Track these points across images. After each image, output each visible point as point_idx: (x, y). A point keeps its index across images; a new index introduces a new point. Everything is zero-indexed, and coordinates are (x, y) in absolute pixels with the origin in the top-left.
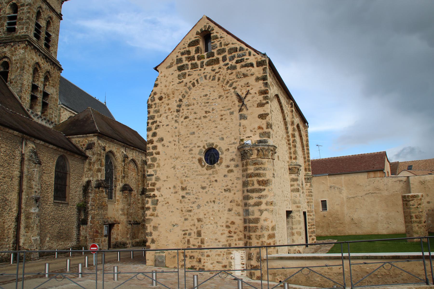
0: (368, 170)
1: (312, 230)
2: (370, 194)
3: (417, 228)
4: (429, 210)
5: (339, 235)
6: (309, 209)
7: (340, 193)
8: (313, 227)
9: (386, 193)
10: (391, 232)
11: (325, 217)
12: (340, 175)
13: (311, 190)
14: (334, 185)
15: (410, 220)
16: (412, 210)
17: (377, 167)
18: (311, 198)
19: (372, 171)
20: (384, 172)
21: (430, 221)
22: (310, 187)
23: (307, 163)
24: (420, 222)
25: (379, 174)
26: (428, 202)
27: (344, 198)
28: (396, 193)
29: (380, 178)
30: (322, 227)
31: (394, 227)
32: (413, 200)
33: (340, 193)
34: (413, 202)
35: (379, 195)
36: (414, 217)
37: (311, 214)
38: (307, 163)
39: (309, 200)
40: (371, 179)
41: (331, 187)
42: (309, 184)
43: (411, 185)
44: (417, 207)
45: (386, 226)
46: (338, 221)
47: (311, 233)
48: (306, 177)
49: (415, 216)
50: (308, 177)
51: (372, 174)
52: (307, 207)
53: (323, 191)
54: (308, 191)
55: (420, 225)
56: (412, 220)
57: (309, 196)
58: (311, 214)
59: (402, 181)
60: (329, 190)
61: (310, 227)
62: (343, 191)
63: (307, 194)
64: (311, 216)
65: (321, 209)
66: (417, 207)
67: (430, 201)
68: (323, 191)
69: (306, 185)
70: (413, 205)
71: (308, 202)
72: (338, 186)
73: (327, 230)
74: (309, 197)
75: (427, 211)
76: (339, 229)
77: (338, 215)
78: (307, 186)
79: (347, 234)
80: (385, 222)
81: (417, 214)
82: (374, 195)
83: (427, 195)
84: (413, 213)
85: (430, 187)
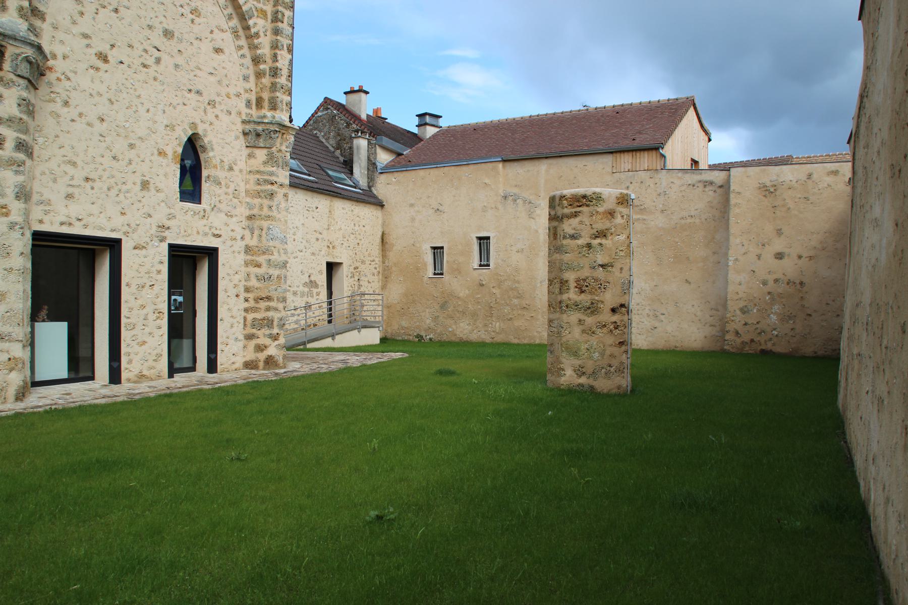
0: (616, 147)
1: (259, 316)
3: (577, 332)
4: (776, 281)
5: (516, 341)
6: (253, 242)
7: (531, 216)
8: (263, 305)
9: (658, 221)
10: (661, 345)
11: (482, 285)
12: (536, 163)
13: (272, 174)
14: (515, 191)
15: (559, 298)
16: (567, 257)
17: (643, 140)
18: (266, 202)
19: (628, 151)
20: (663, 156)
21: (774, 317)
22: (265, 163)
23: (266, 81)
24: (592, 309)
25: (646, 160)
26: (779, 256)
27: (540, 231)
28: (689, 220)
29: (649, 173)
30: (474, 315)
31: (669, 329)
32: (575, 215)
33: (531, 216)
34: (574, 222)
36: (572, 284)
37: (261, 259)
38: (266, 81)
39: (255, 211)
40: (623, 176)
41: (505, 197)
42: (261, 154)
44: (589, 246)
46: (516, 301)
47: (253, 326)
48: (248, 127)
49: (577, 281)
50: (260, 128)
51: (626, 161)
52: (247, 233)
53: (485, 209)
54: (253, 178)
55: (590, 320)
56: (565, 297)
57: (258, 194)
58: (261, 259)
59: (711, 183)
60: (500, 206)
61: (252, 303)
62: (538, 211)
63: (252, 186)
64: (259, 266)
65: (476, 263)
66: (589, 246)
67: (786, 251)
68: (485, 209)
69: (250, 156)
70: (573, 237)
71: (250, 218)
72: (526, 195)
73: (486, 325)
74: (257, 201)
75: (771, 283)
76: (517, 323)
77: (518, 282)
78: (252, 161)
79: (537, 342)
80: (647, 311)
81: (586, 273)
83: (779, 232)
84: (570, 268)
85: (791, 205)
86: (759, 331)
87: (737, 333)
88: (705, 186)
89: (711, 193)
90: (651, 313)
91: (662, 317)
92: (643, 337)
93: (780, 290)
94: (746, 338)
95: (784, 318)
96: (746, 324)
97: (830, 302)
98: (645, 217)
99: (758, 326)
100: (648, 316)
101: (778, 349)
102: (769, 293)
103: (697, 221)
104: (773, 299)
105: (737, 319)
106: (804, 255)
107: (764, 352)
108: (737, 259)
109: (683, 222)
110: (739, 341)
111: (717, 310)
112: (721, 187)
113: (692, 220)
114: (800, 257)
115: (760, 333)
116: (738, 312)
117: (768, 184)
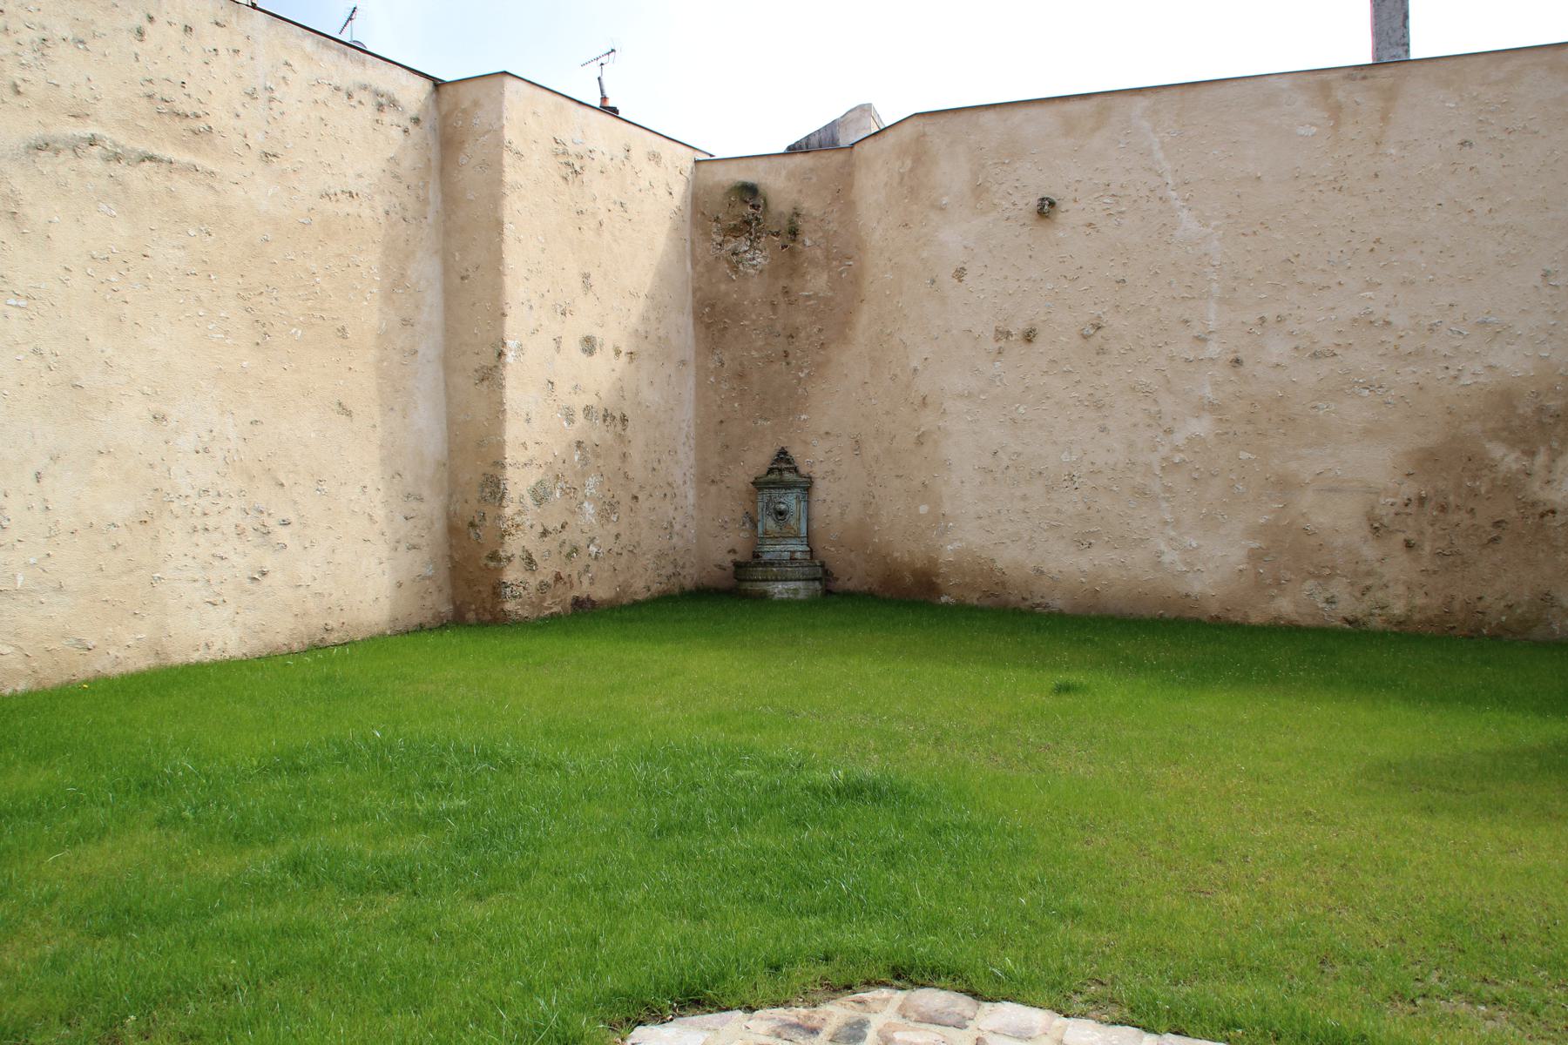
2: (92, 162)
4: (588, 410)
10: (282, 631)
21: (589, 508)
35: (193, 195)
43: (508, 158)
45: (242, 558)
75: (580, 417)
80: (234, 517)
82: (136, 176)
86: (567, 549)
87: (530, 561)
88: (380, 107)
89: (396, 133)
90: (248, 523)
91: (283, 534)
92: (226, 612)
93: (595, 438)
94: (546, 572)
95: (608, 509)
96: (545, 533)
97: (655, 465)
98: (199, 161)
99: (564, 536)
100: (240, 534)
101: (601, 592)
102: (579, 444)
103: (366, 212)
104: (584, 460)
105: (527, 520)
106: (624, 349)
107: (578, 603)
108: (520, 347)
109: (329, 206)
110: (533, 582)
111: (421, 500)
112: (416, 121)
113: (346, 207)
114: (618, 352)
115: (569, 556)
116: (529, 501)
117: (571, 149)
